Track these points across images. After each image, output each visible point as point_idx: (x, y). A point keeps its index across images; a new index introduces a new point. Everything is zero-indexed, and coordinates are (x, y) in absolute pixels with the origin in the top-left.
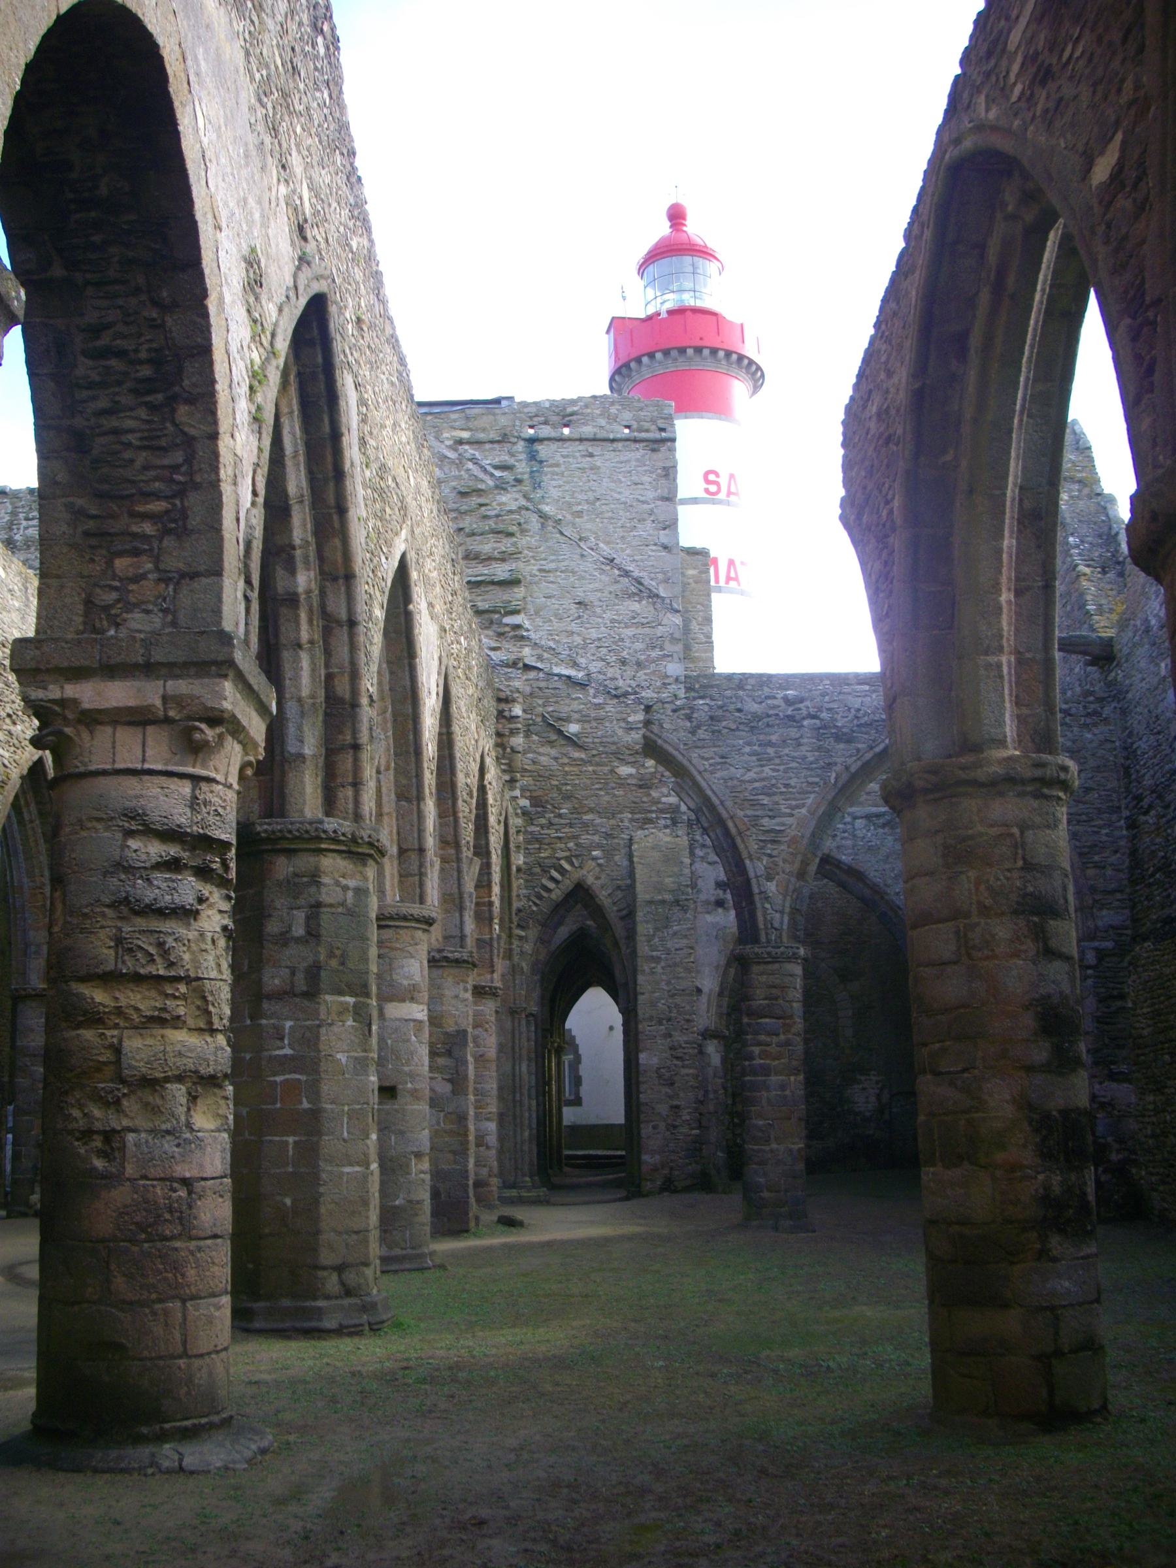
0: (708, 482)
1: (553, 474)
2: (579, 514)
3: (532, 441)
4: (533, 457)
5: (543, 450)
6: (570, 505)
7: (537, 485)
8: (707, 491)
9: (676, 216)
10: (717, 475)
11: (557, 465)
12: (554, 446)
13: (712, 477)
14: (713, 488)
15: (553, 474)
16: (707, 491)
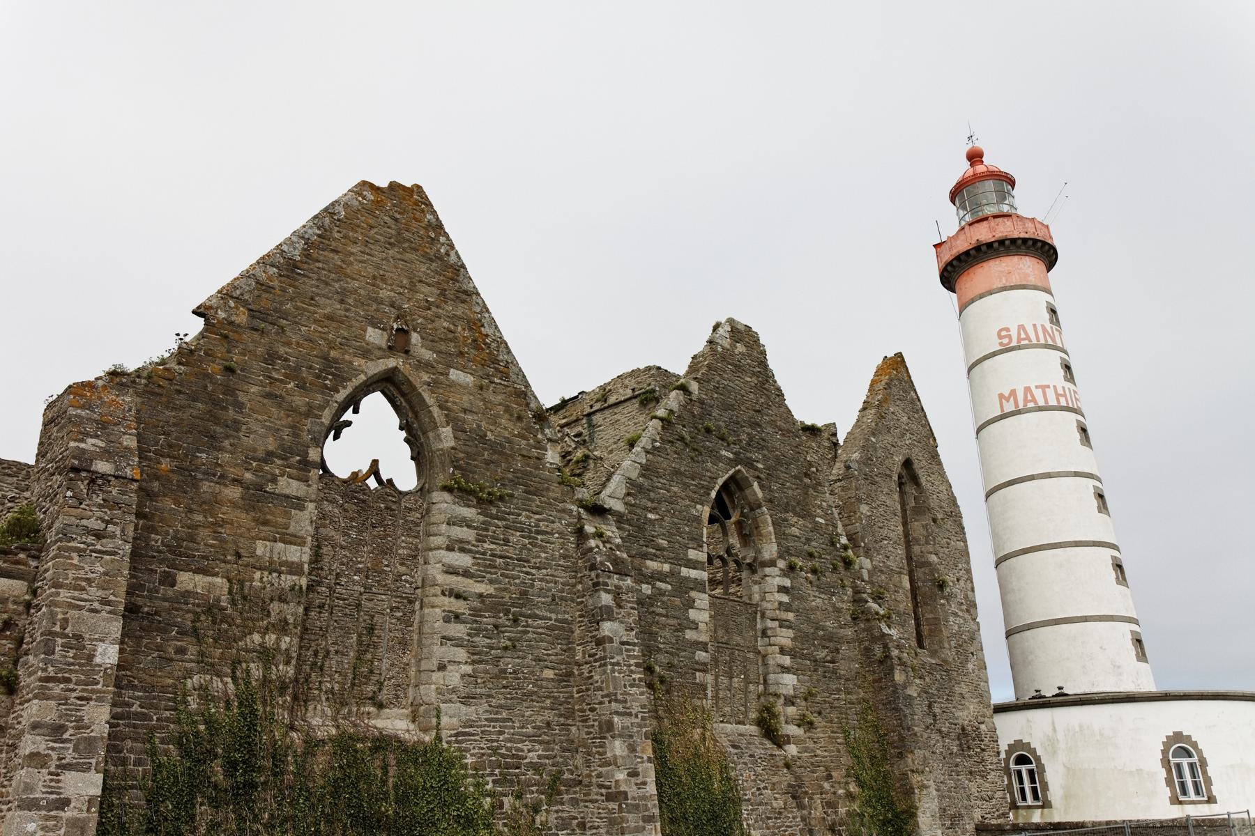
0: (1000, 337)
1: (600, 431)
2: (611, 452)
3: (589, 415)
4: (591, 426)
5: (597, 419)
6: (607, 448)
7: (592, 440)
8: (1001, 344)
9: (975, 157)
10: (1008, 330)
11: (600, 426)
12: (598, 415)
13: (1004, 333)
14: (1006, 341)
15: (600, 431)
16: (1001, 344)
